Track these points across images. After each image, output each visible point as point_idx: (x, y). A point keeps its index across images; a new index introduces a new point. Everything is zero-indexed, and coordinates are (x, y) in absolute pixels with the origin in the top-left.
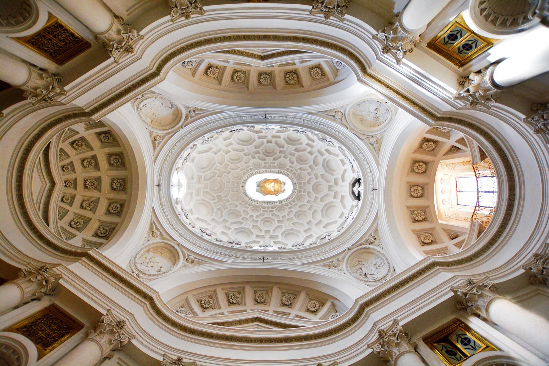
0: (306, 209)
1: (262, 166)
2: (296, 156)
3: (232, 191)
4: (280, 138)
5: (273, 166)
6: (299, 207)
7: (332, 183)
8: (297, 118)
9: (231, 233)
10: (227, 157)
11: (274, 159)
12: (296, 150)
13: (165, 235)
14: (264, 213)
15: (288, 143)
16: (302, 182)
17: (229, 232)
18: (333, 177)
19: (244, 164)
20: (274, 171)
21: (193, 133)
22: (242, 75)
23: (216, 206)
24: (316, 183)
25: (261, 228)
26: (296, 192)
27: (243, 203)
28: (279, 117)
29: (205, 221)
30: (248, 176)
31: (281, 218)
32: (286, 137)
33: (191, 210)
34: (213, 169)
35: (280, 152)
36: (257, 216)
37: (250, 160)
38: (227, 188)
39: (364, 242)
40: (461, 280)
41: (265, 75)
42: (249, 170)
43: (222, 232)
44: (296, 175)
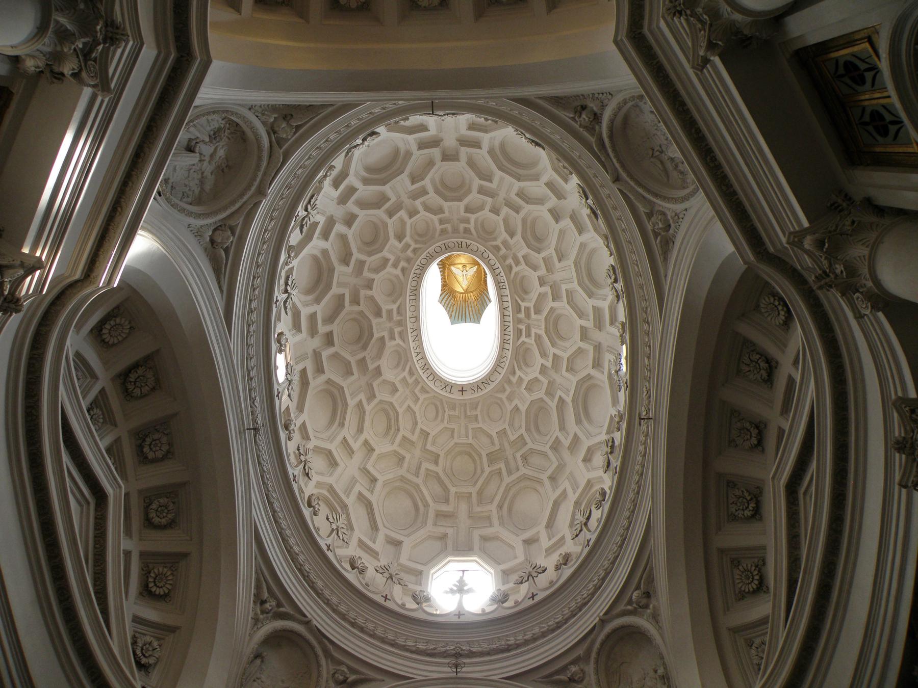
0: (517, 220)
1: (401, 343)
2: (363, 257)
3: (477, 420)
4: (315, 313)
5: (398, 313)
6: (512, 238)
7: (436, 152)
8: (248, 332)
9: (588, 438)
10: (382, 447)
11: (378, 314)
12: (345, 261)
13: (580, 651)
14: (533, 335)
15: (329, 287)
16: (439, 227)
17: (586, 443)
18: (417, 153)
19: (398, 394)
20: (412, 309)
21: (320, 584)
22: (154, 506)
23: (518, 469)
24: (437, 192)
25: (574, 349)
26: (469, 242)
27: (508, 390)
28: (251, 379)
29: (556, 505)
30: (431, 378)
31: (546, 289)
32: (310, 298)
33: (528, 542)
34: (415, 480)
35: (356, 301)
36: (544, 354)
37: (384, 381)
38: (467, 437)
39: (593, 135)
41: (146, 449)
42: (414, 378)
43: (584, 460)
44: (418, 246)
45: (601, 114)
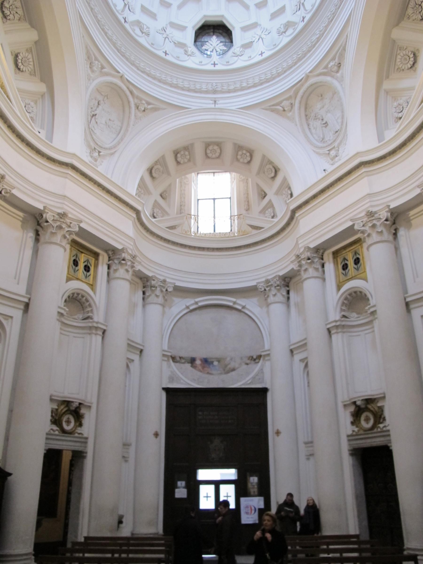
40: (132, 246)
45: (135, 110)
